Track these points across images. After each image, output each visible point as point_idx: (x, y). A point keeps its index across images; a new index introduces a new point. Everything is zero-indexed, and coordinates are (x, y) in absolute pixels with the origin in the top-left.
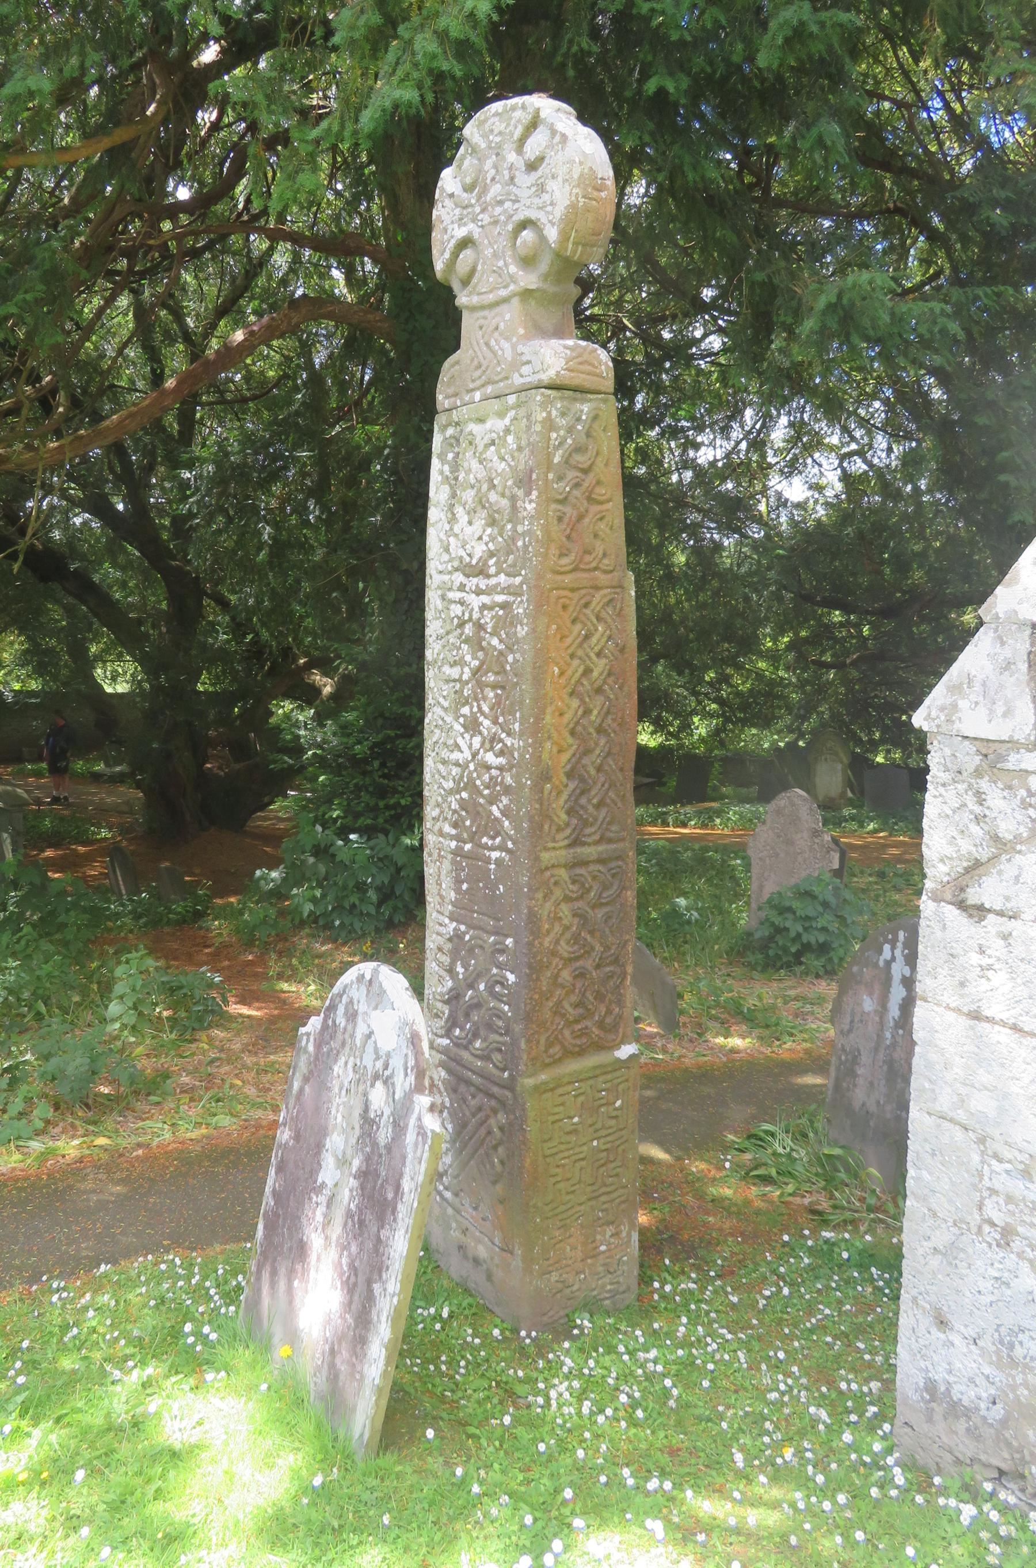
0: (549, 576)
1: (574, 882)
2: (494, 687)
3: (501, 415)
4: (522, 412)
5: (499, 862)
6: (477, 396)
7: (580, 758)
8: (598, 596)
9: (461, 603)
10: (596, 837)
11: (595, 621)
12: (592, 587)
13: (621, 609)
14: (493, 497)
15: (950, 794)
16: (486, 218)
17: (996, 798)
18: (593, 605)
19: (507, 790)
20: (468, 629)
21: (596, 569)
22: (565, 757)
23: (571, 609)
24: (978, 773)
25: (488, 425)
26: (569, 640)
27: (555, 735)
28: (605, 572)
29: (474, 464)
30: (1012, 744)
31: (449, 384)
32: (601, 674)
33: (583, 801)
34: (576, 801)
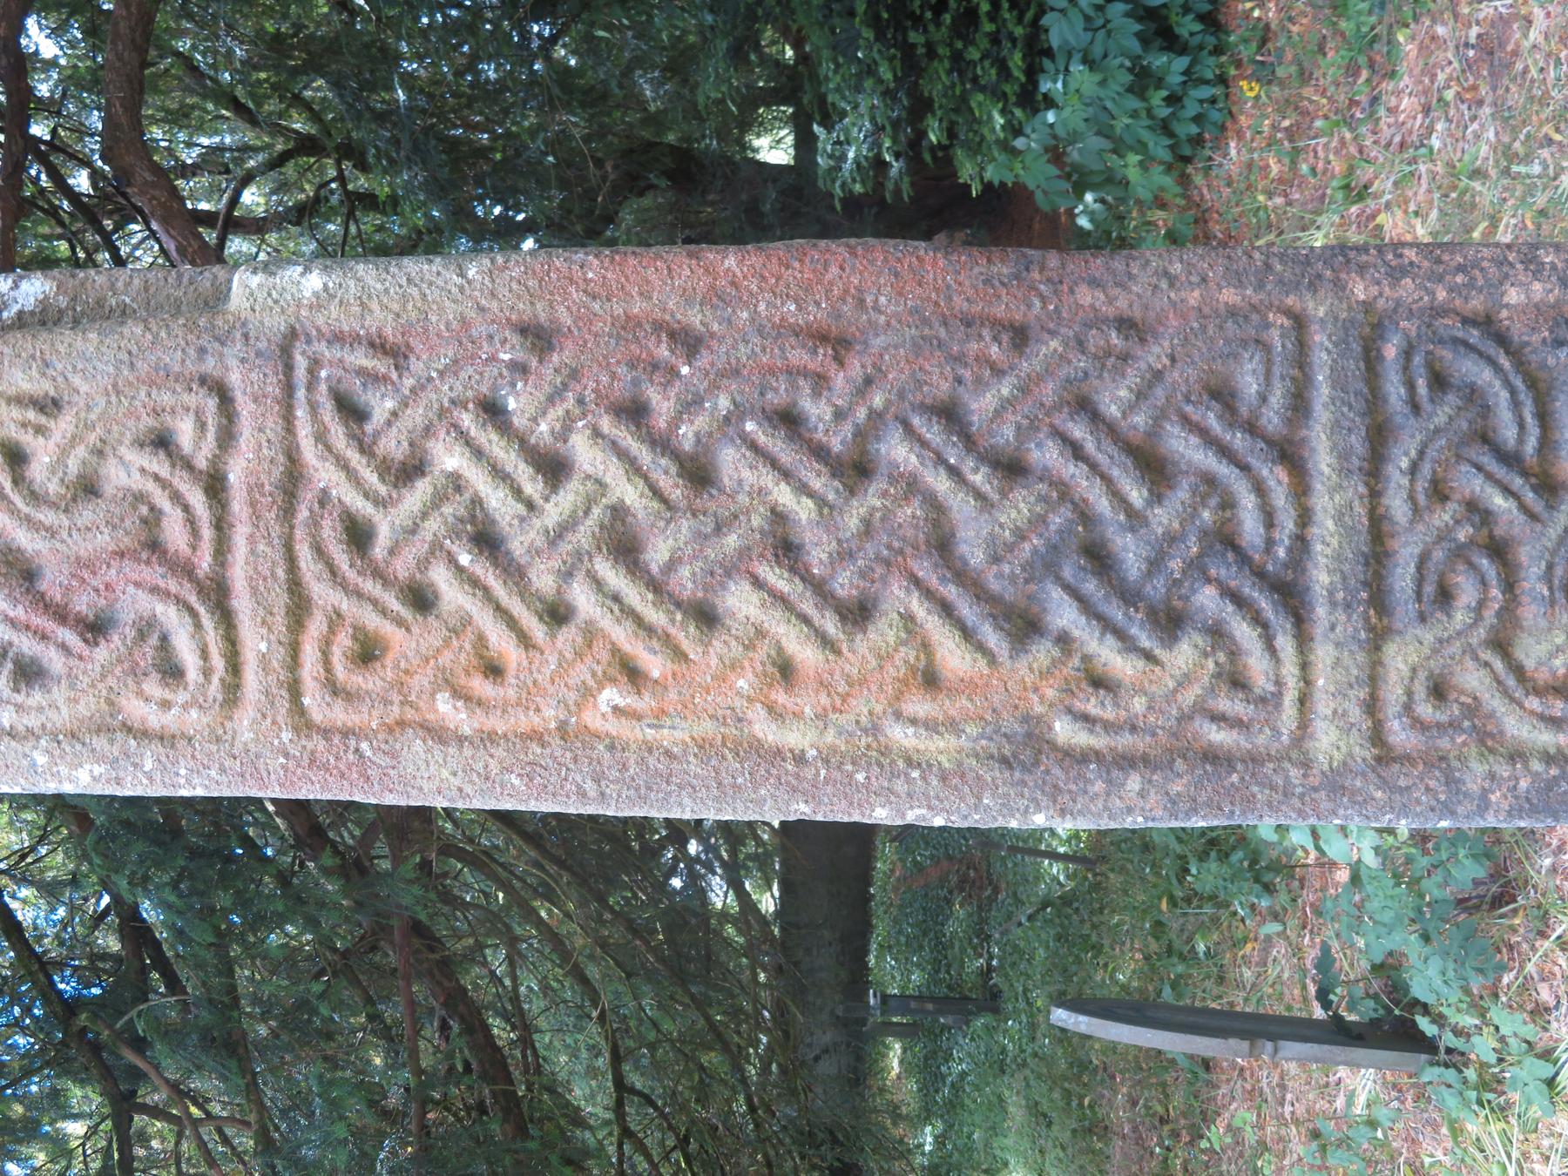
0: (244, 723)
1: (1445, 596)
7: (962, 576)
8: (324, 474)
10: (1277, 479)
11: (422, 489)
12: (288, 512)
13: (379, 346)
18: (360, 505)
21: (215, 486)
22: (954, 657)
23: (372, 620)
26: (500, 640)
27: (861, 707)
28: (227, 437)
32: (633, 467)
33: (1131, 553)
34: (1129, 596)
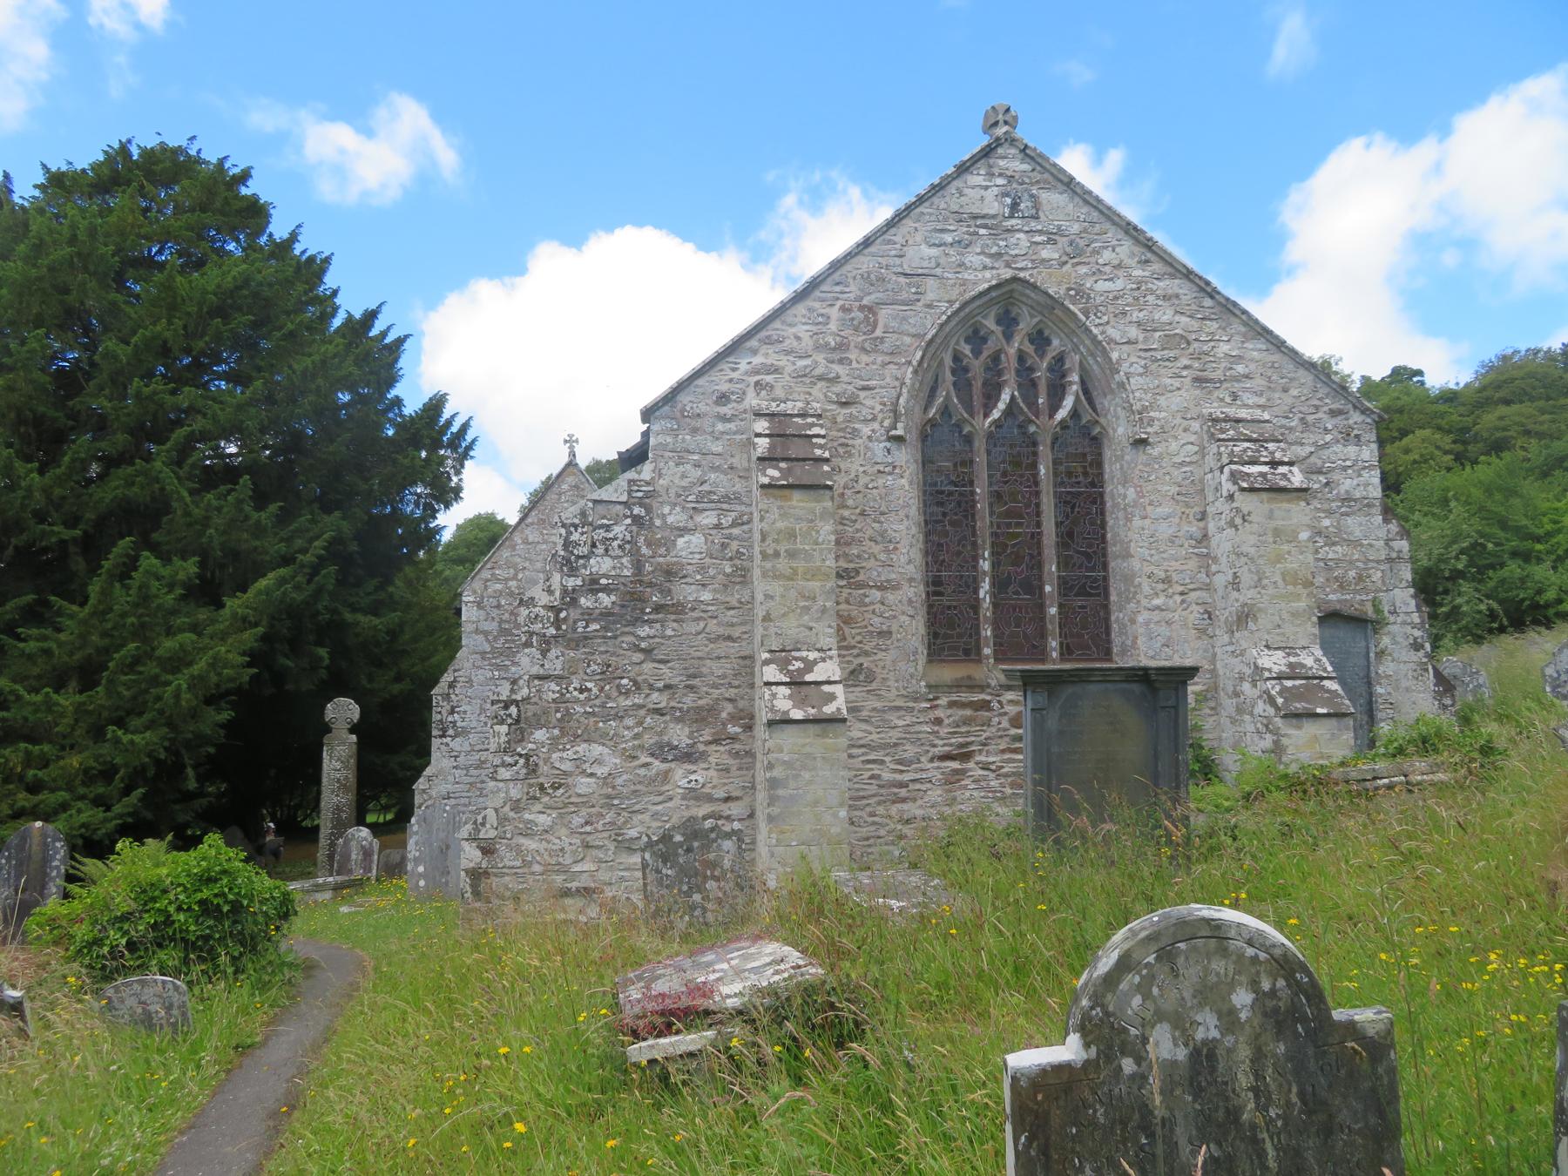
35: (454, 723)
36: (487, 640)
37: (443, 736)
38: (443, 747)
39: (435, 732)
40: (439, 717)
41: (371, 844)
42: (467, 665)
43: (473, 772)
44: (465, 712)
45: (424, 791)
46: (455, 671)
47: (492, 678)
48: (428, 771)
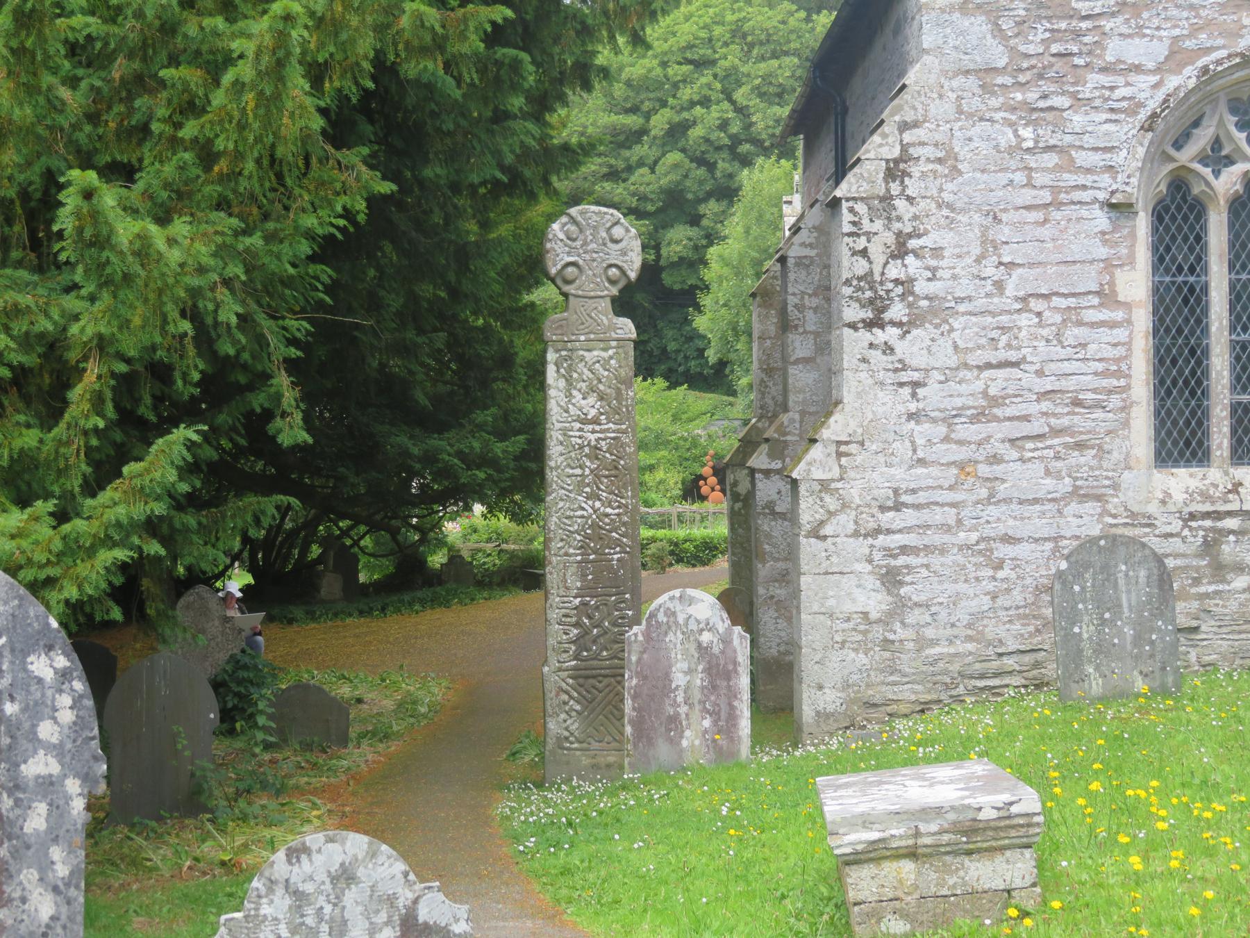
2: (606, 477)
3: (605, 350)
4: (620, 351)
5: (618, 560)
6: (582, 338)
9: (580, 437)
14: (601, 387)
15: (810, 500)
16: (588, 257)
17: (827, 498)
19: (624, 524)
20: (587, 450)
24: (820, 491)
25: (595, 353)
29: (585, 371)
30: (833, 480)
31: (557, 328)
35: (906, 284)
36: (998, 31)
37: (875, 323)
38: (876, 355)
39: (853, 313)
40: (861, 266)
41: (726, 641)
42: (941, 109)
43: (965, 431)
44: (937, 252)
45: (825, 485)
46: (904, 127)
47: (1016, 149)
48: (836, 427)
